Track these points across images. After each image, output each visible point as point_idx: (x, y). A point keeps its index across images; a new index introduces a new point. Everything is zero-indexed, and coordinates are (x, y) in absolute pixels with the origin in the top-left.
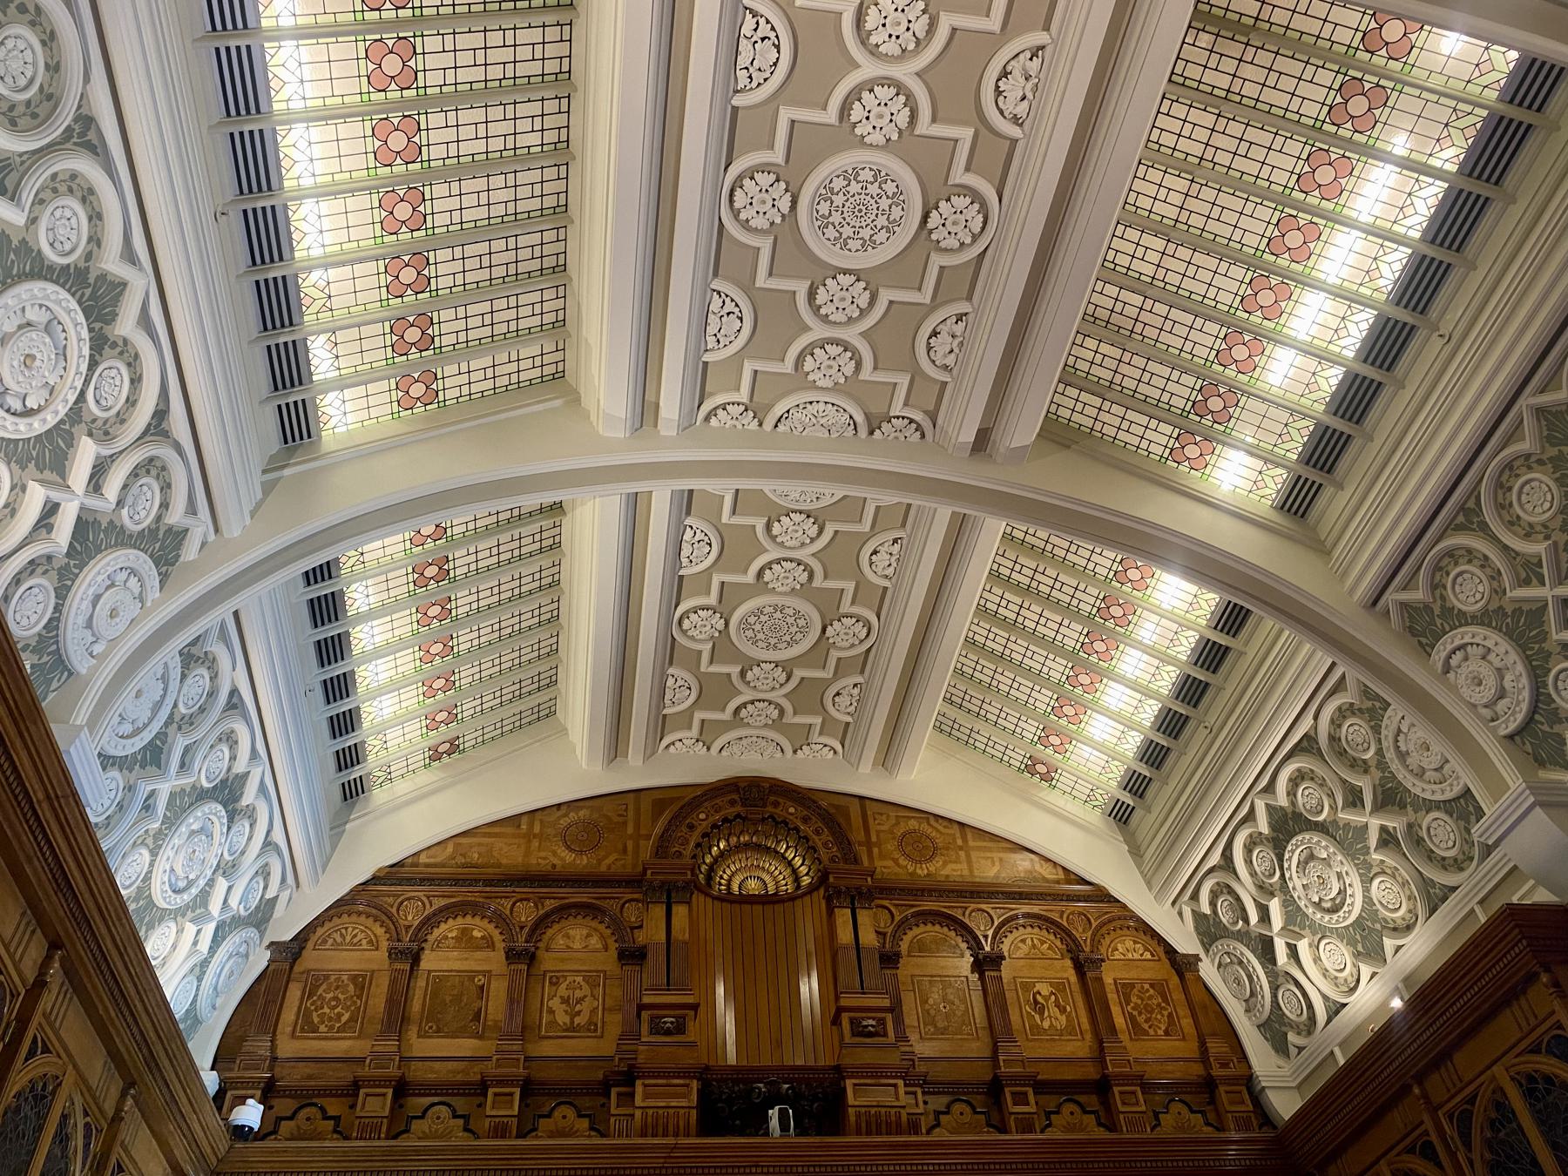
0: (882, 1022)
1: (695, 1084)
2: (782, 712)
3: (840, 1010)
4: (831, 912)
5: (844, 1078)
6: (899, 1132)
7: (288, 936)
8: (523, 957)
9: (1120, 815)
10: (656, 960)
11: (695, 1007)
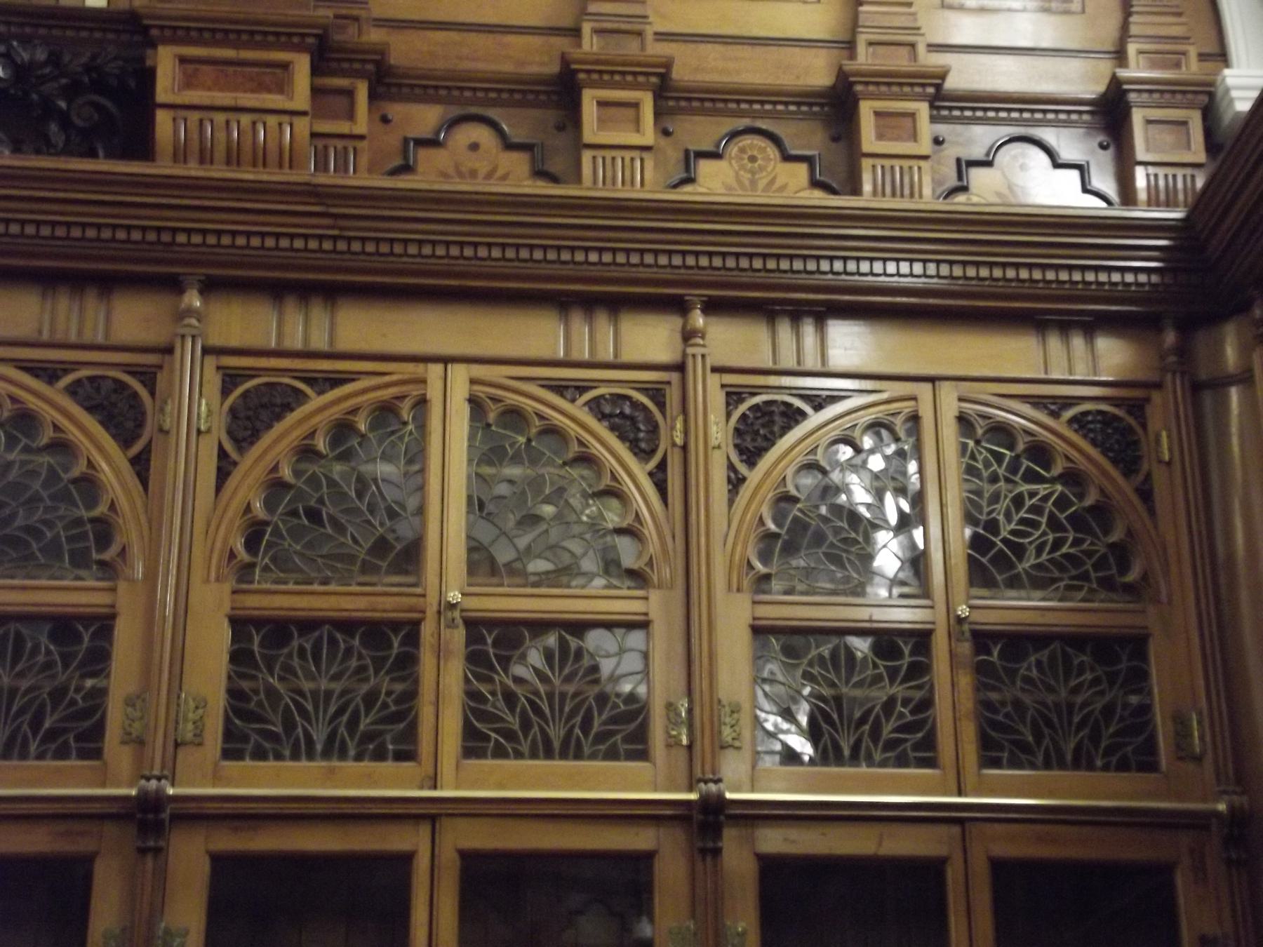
5: (153, 45)
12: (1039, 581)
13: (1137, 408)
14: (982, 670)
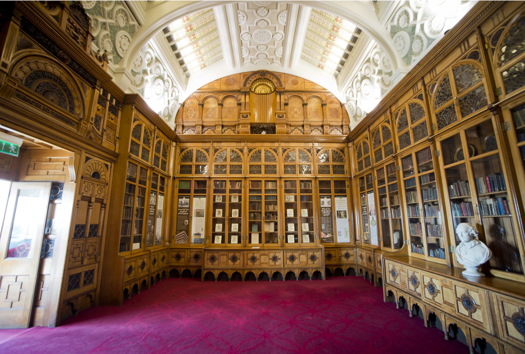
0: (283, 115)
1: (249, 126)
2: (267, 56)
3: (276, 113)
4: (276, 95)
6: (285, 134)
7: (182, 102)
8: (221, 105)
9: (336, 76)
10: (243, 105)
11: (250, 113)
12: (337, 161)
13: (344, 149)
14: (333, 168)
